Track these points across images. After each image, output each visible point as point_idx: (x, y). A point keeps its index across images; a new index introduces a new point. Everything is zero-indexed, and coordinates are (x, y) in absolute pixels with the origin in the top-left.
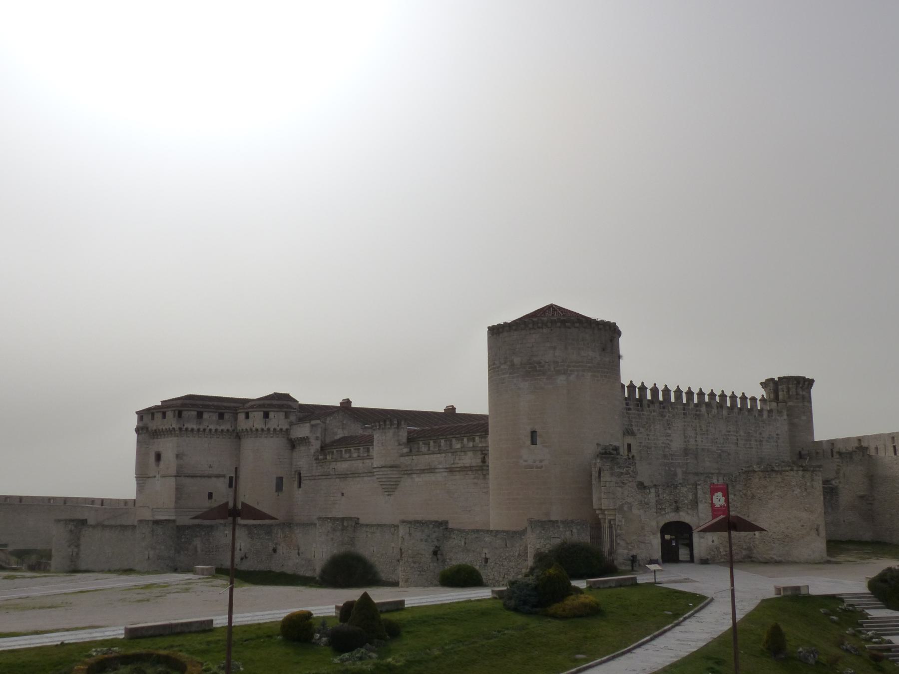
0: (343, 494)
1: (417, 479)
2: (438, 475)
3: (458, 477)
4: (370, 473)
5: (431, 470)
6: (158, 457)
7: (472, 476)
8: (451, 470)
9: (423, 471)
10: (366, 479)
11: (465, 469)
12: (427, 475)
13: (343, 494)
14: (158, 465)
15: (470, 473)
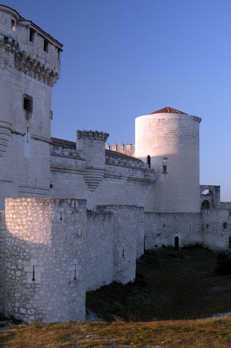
0: (51, 186)
1: (110, 182)
2: (122, 180)
3: (131, 183)
4: (80, 171)
5: (120, 177)
6: (28, 104)
7: (138, 185)
8: (130, 179)
9: (115, 177)
10: (73, 175)
11: (136, 180)
12: (116, 180)
13: (51, 186)
14: (28, 118)
15: (137, 182)
